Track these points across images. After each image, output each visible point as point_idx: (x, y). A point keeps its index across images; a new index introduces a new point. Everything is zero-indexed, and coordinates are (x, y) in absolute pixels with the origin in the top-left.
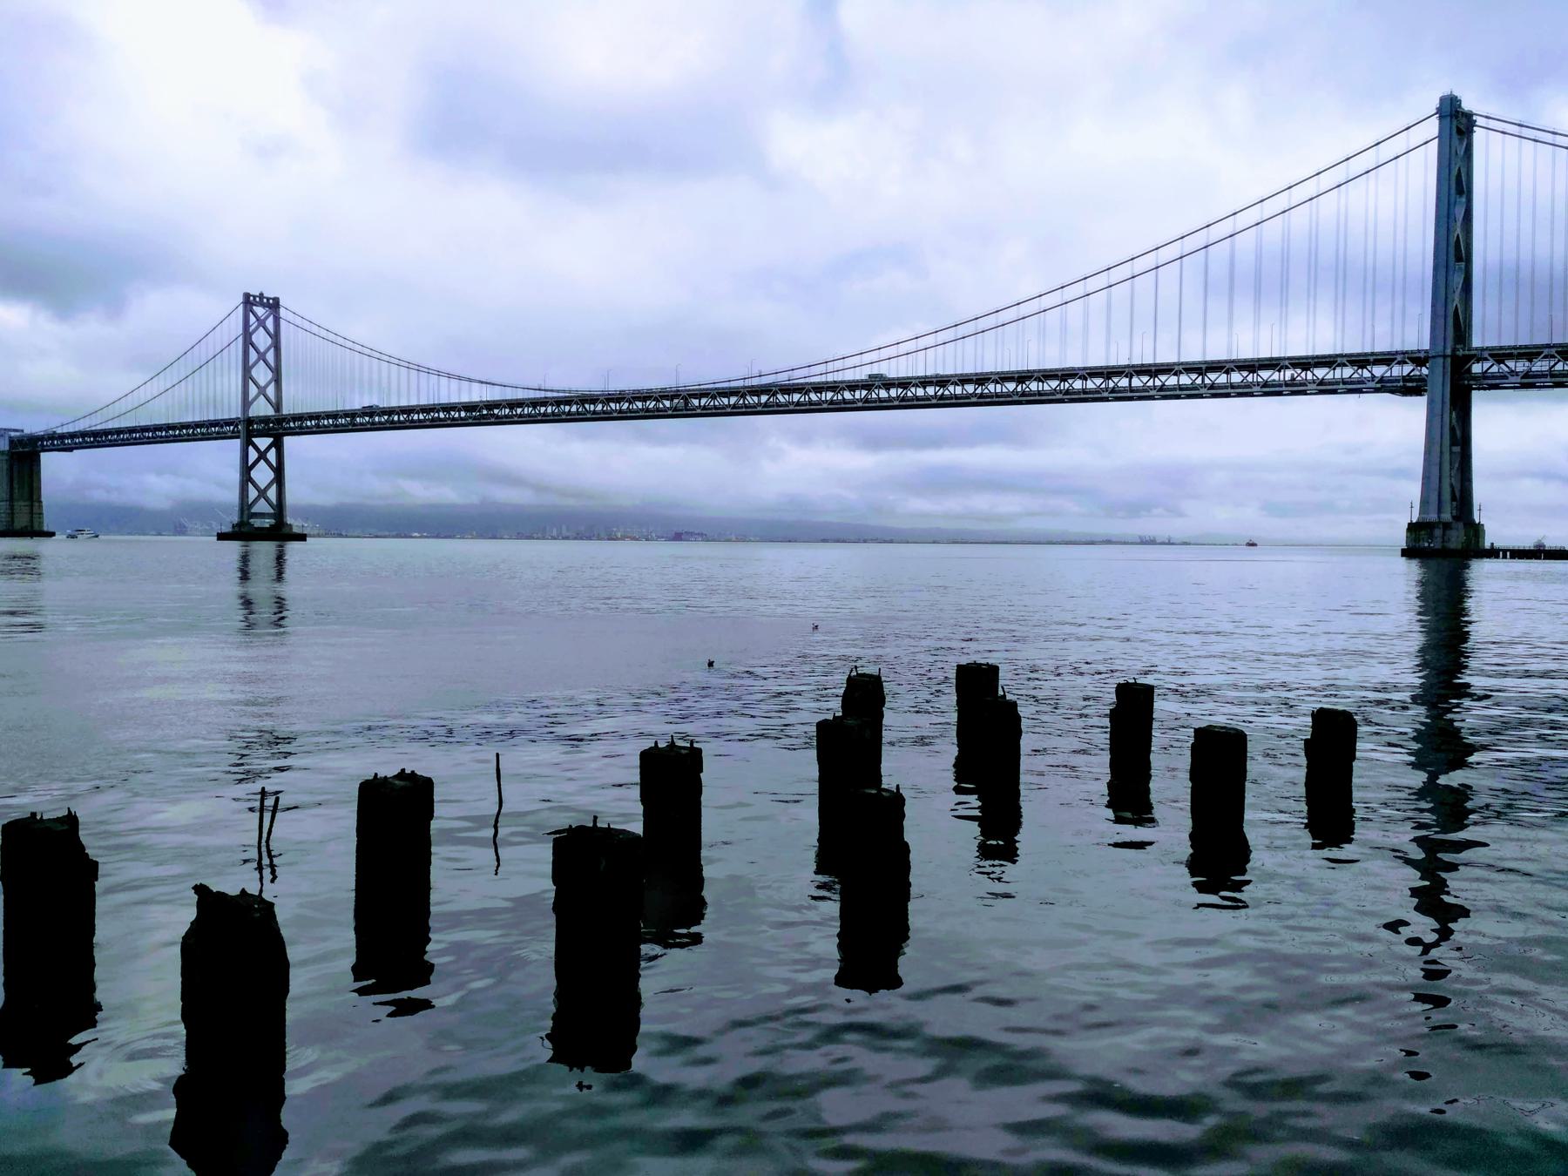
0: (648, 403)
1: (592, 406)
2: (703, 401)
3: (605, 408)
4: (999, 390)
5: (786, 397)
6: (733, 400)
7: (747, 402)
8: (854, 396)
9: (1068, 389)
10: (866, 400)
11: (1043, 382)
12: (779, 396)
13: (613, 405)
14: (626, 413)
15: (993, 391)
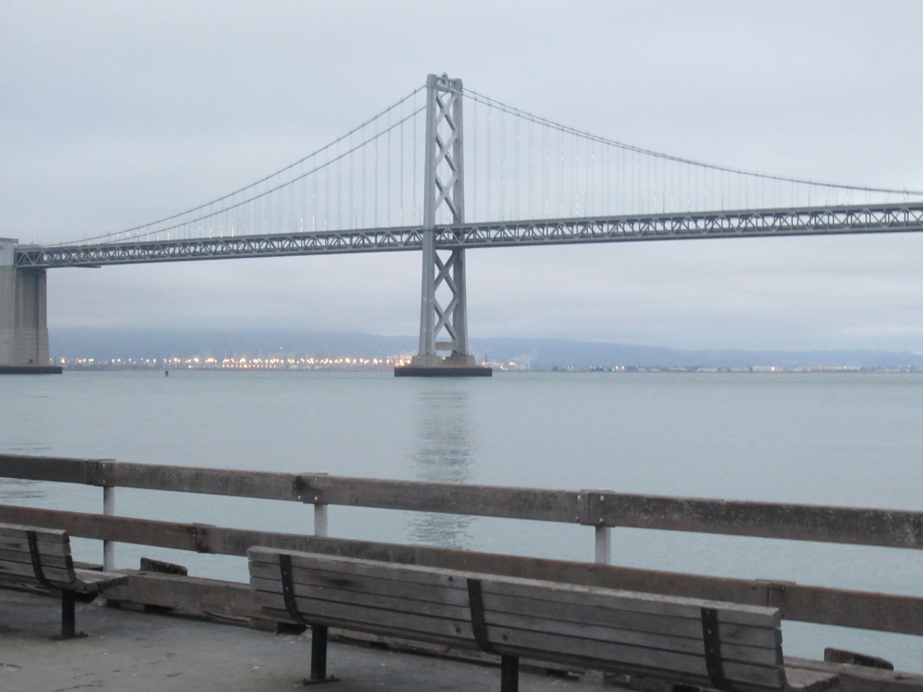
0: (307, 241)
1: (257, 244)
2: (379, 238)
3: (246, 248)
4: (795, 223)
5: (513, 231)
6: (405, 237)
7: (477, 237)
8: (602, 230)
9: (893, 221)
10: (582, 235)
11: (908, 213)
12: (506, 231)
13: (276, 243)
14: (287, 250)
15: (790, 223)
